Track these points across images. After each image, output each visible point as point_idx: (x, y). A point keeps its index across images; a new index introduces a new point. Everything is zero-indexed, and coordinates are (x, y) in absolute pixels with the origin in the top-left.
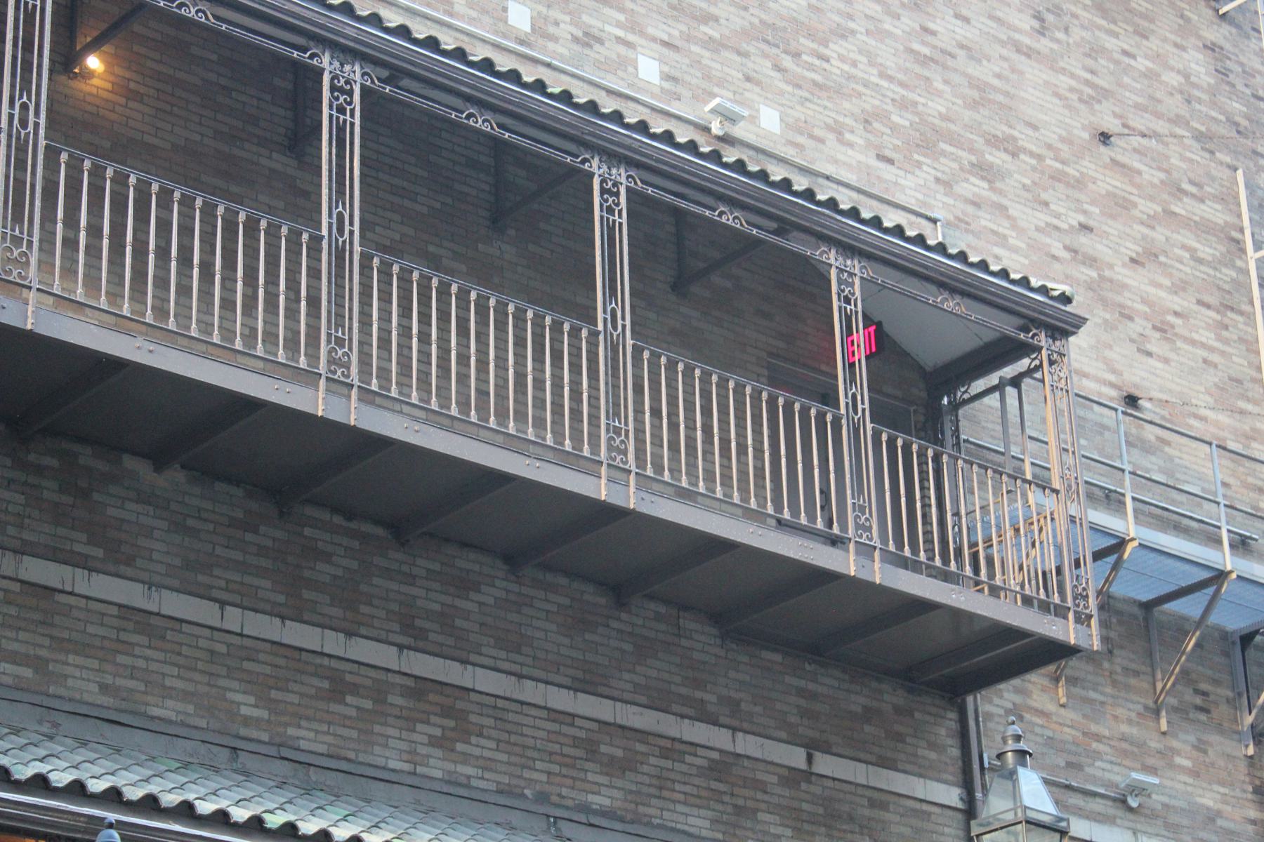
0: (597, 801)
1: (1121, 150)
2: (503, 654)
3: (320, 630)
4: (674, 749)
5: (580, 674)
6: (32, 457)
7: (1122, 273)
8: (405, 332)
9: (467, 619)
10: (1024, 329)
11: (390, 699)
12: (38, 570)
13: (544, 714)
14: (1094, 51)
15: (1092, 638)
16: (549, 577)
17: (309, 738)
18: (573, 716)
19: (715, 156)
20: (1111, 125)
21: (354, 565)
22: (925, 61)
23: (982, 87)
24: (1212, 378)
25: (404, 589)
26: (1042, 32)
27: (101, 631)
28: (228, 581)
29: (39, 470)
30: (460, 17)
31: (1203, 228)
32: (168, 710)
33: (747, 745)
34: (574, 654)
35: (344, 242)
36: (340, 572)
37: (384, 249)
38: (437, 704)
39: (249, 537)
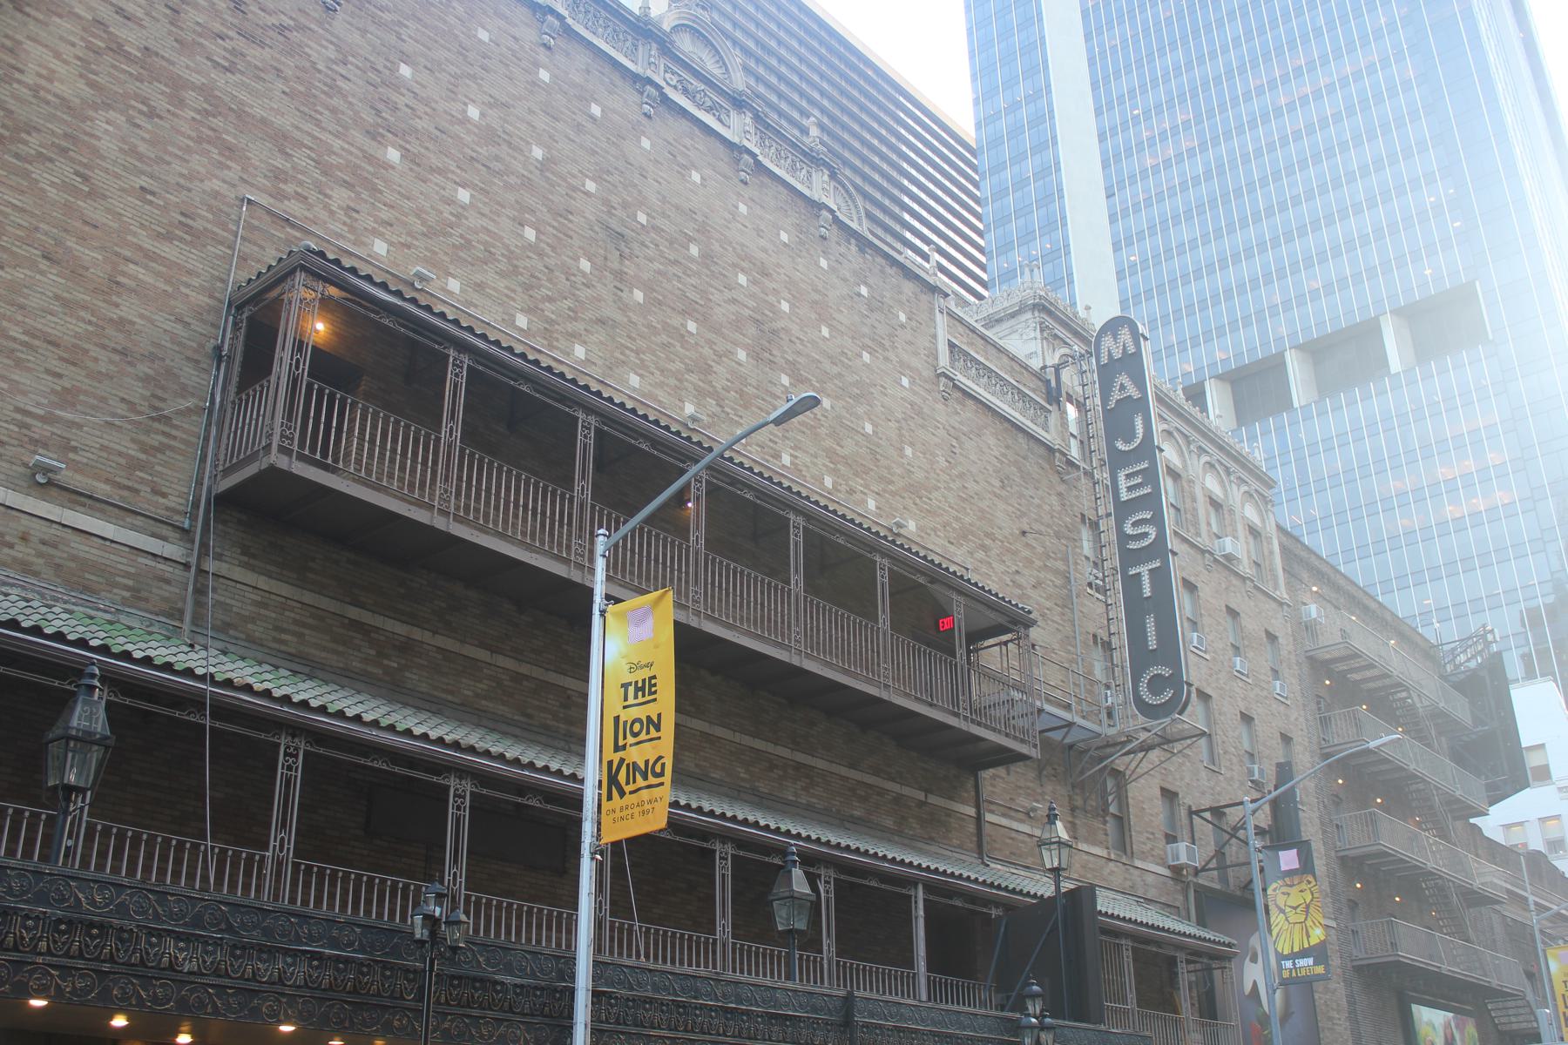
0: (857, 813)
1: (1030, 539)
4: (882, 792)
7: (1030, 592)
10: (1009, 622)
14: (1021, 496)
15: (1035, 753)
17: (763, 787)
19: (893, 542)
20: (1026, 528)
22: (964, 500)
23: (982, 511)
24: (1059, 636)
26: (1003, 487)
31: (1056, 572)
32: (716, 775)
33: (906, 791)
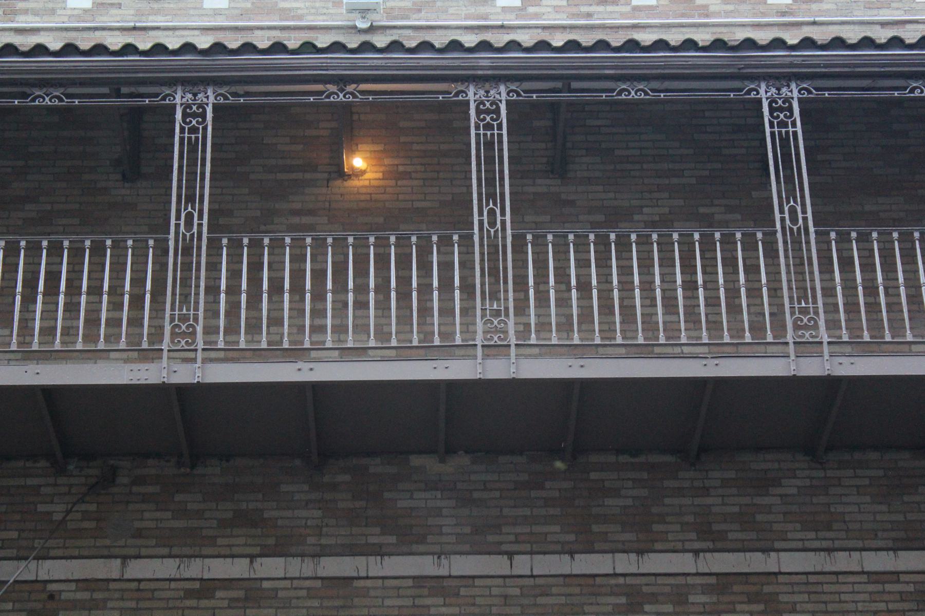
2: (812, 535)
3: (611, 555)
5: (902, 534)
6: (326, 479)
8: (626, 287)
9: (770, 513)
11: (691, 599)
12: (333, 566)
13: (864, 578)
16: (857, 455)
18: (898, 573)
21: (644, 492)
25: (698, 501)
27: (399, 602)
28: (516, 535)
29: (334, 487)
30: (717, 14)
34: (894, 517)
35: (799, 229)
36: (629, 502)
37: (653, 225)
38: (743, 593)
39: (534, 494)
